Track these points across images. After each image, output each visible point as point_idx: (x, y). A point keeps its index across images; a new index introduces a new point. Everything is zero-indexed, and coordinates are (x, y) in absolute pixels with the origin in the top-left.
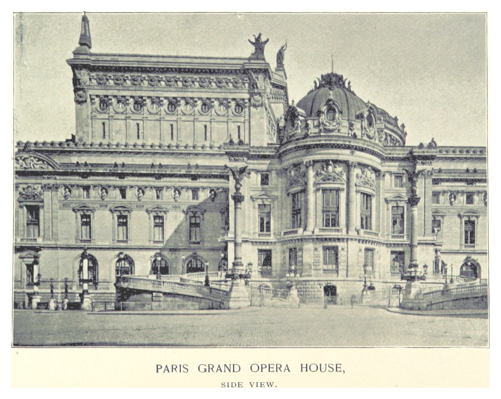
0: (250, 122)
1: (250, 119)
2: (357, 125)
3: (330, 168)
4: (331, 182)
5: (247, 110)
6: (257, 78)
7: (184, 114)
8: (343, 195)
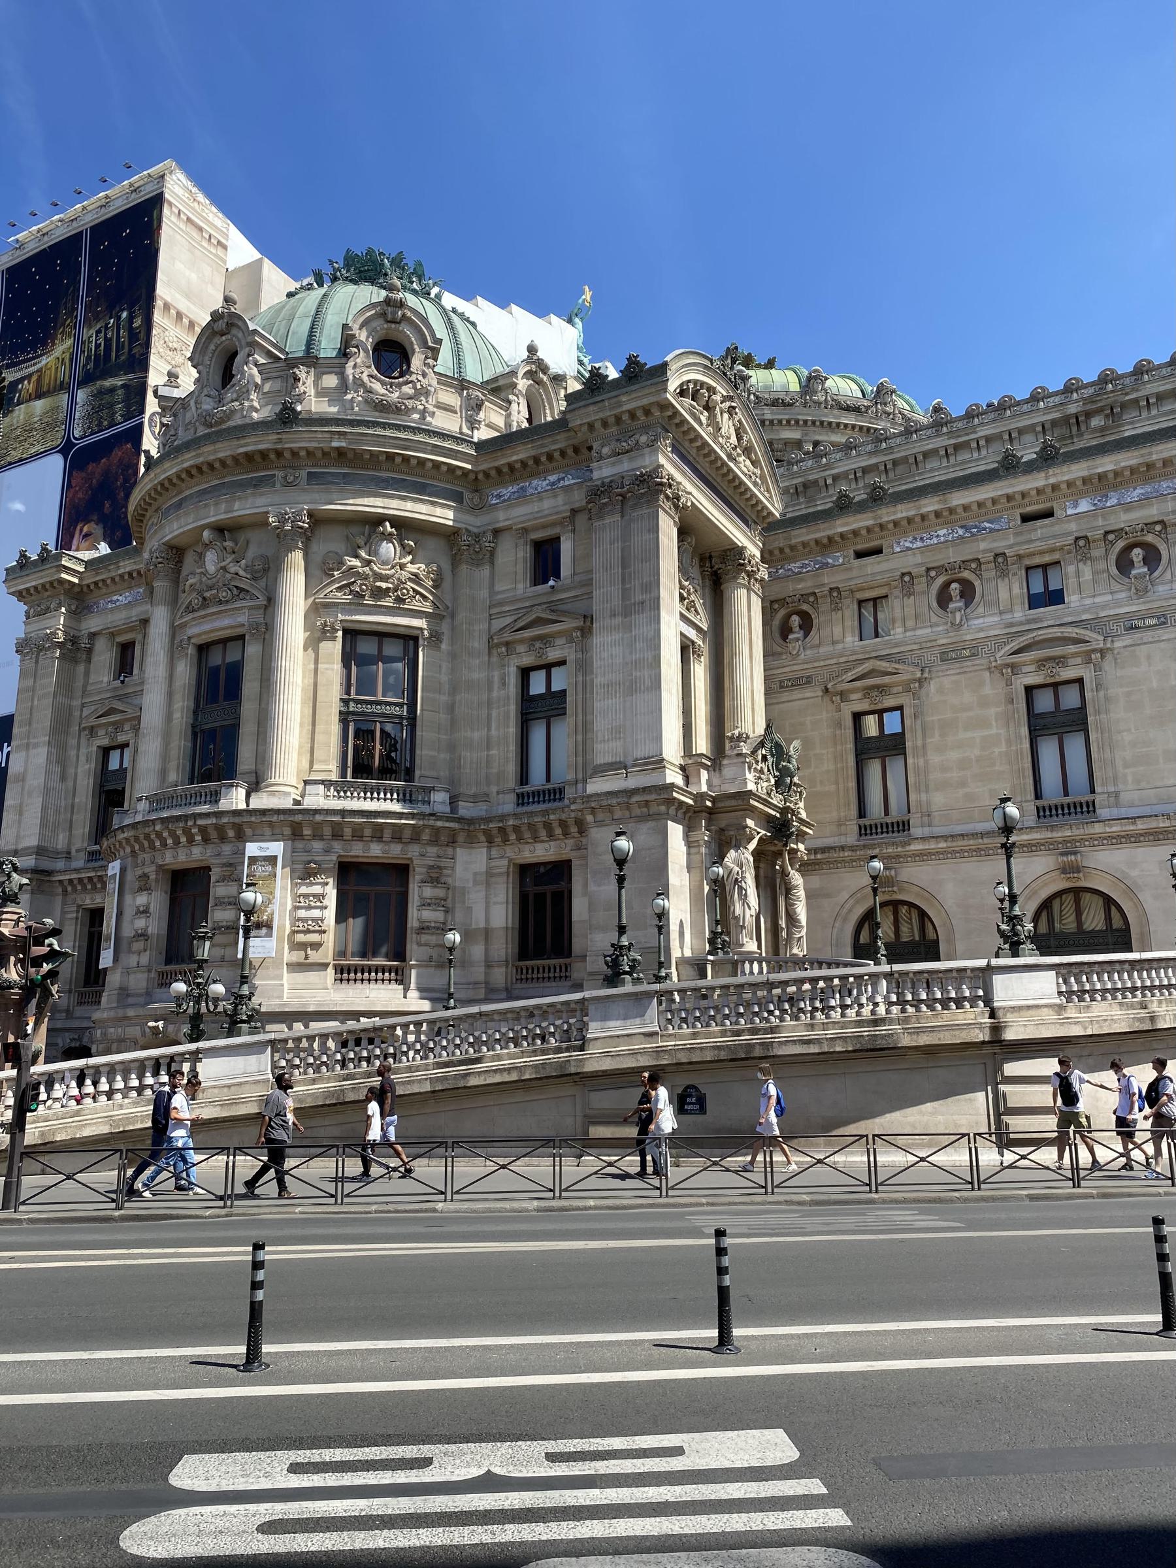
4: (388, 602)
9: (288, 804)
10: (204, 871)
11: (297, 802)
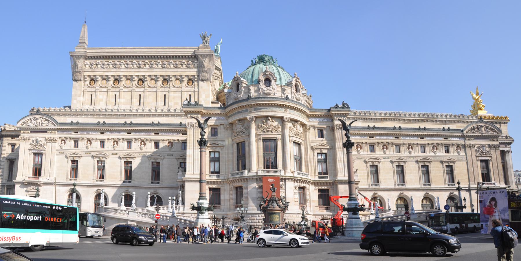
0: (198, 92)
2: (288, 91)
3: (269, 122)
4: (270, 133)
6: (204, 61)
8: (279, 144)
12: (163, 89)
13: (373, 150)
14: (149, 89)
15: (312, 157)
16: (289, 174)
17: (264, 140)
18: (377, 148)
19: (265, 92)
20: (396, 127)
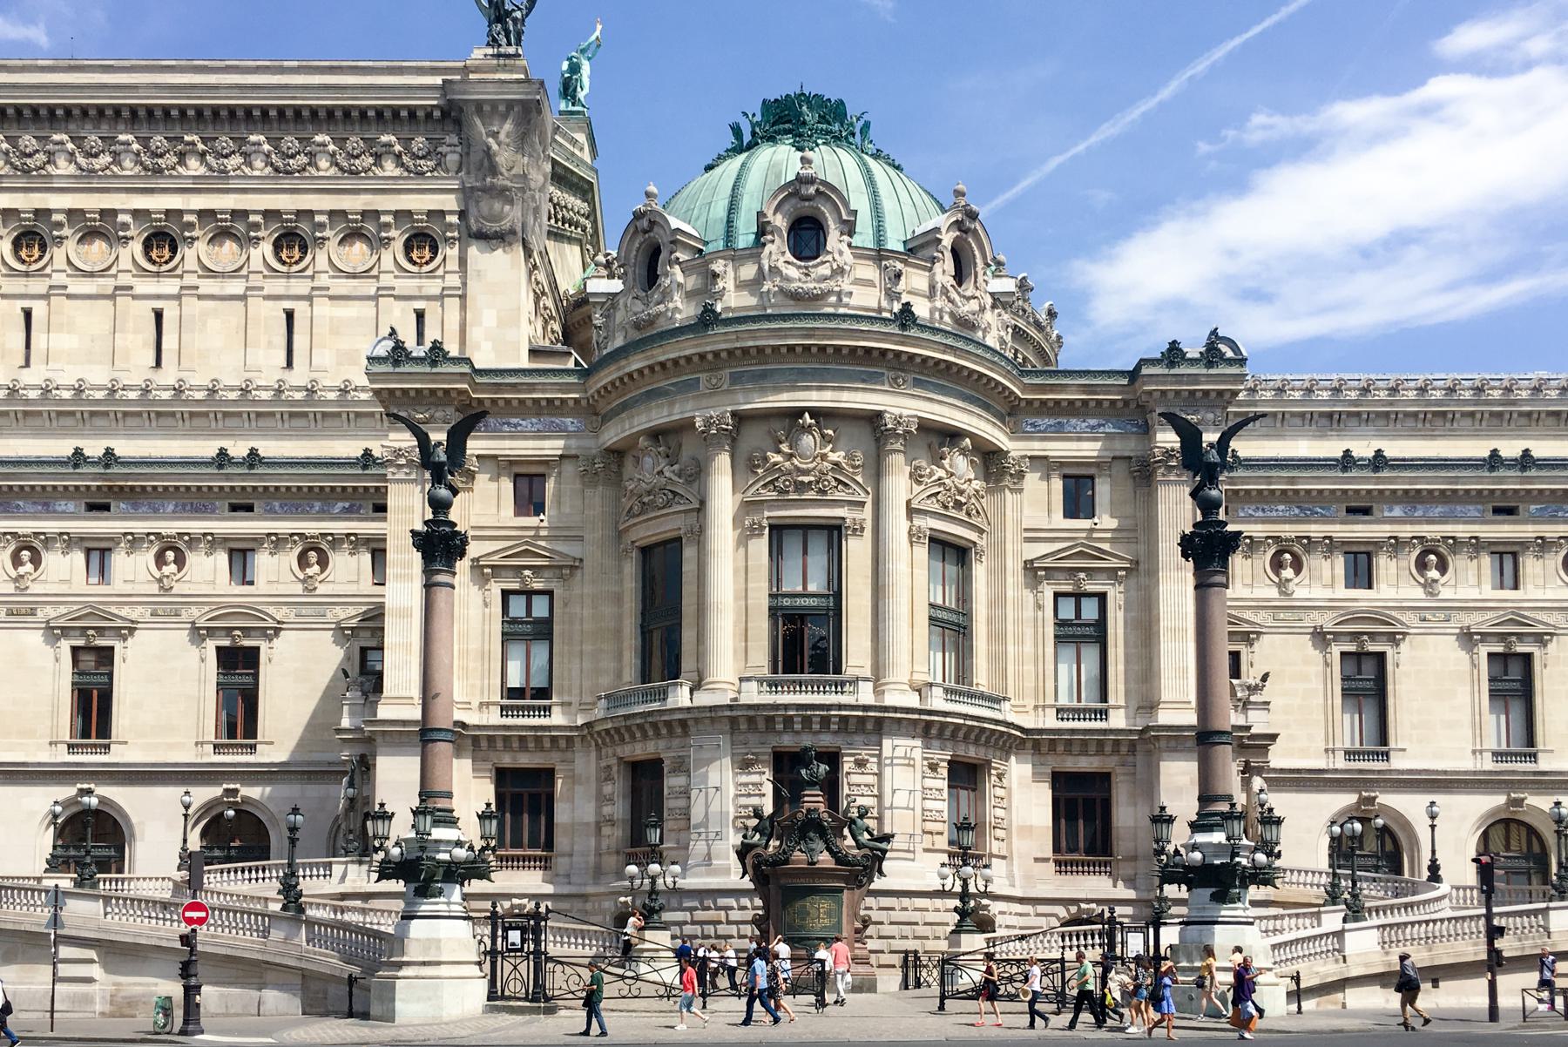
0: (463, 297)
1: (464, 284)
4: (811, 495)
5: (452, 252)
6: (495, 135)
7: (209, 273)
8: (857, 551)
9: (724, 699)
10: (658, 762)
11: (735, 699)
12: (276, 286)
13: (1361, 571)
14: (208, 286)
15: (1029, 613)
16: (900, 697)
17: (778, 531)
18: (1385, 566)
19: (793, 286)
20: (1504, 453)
